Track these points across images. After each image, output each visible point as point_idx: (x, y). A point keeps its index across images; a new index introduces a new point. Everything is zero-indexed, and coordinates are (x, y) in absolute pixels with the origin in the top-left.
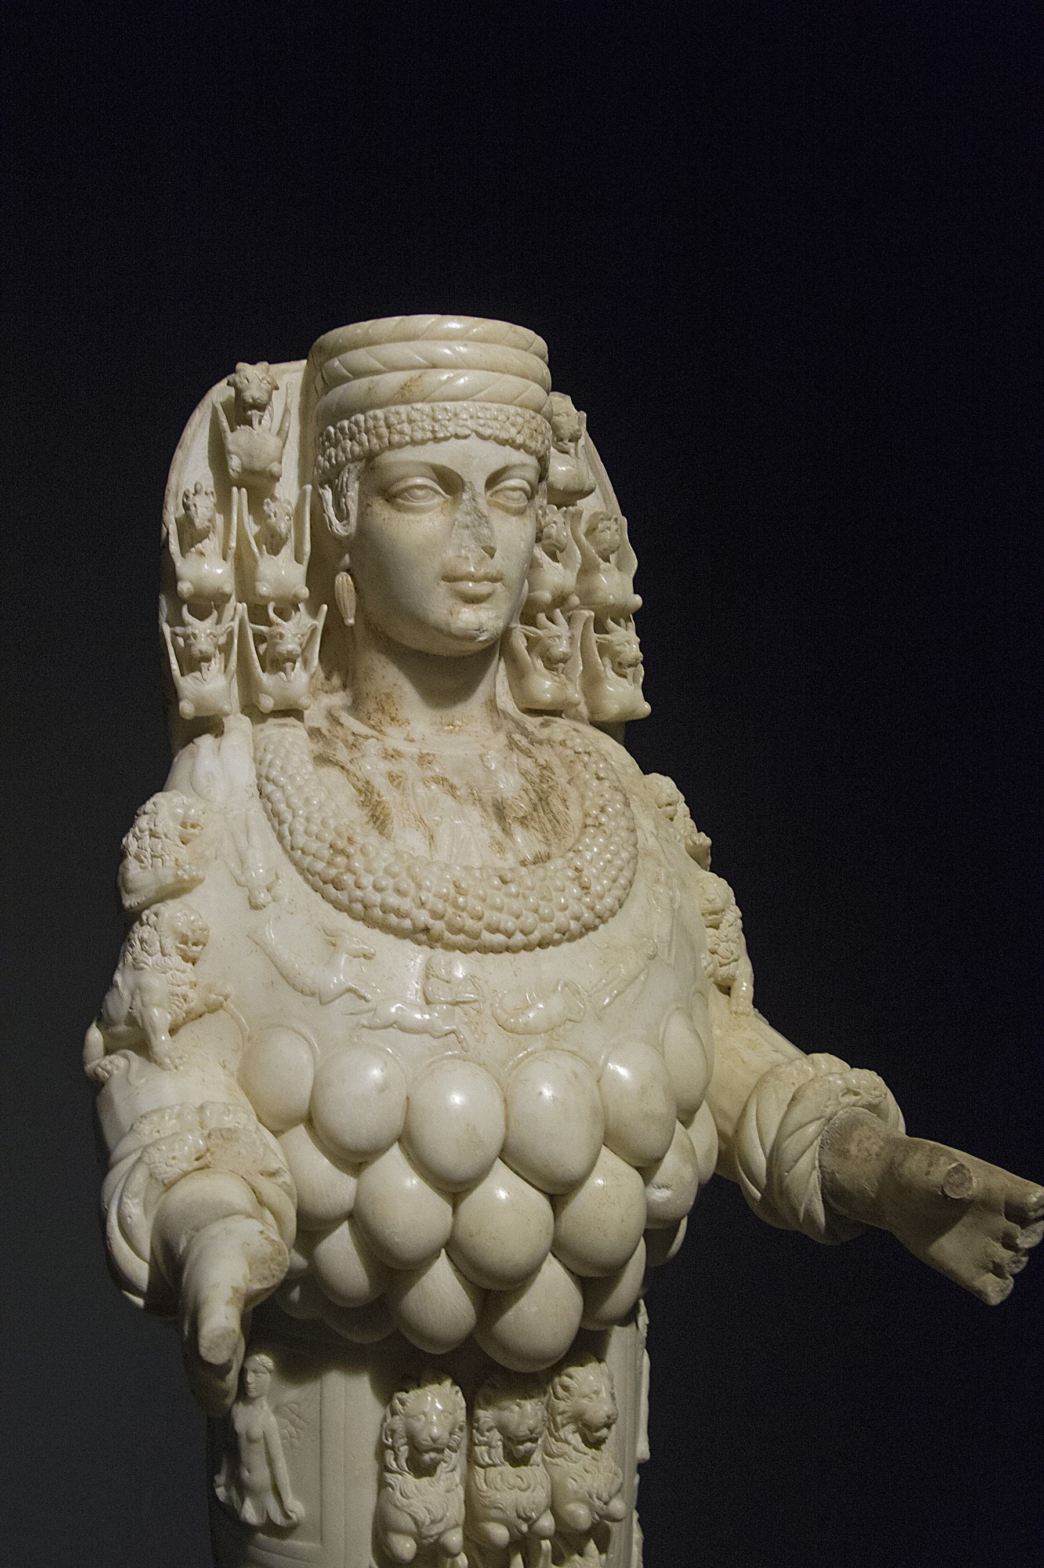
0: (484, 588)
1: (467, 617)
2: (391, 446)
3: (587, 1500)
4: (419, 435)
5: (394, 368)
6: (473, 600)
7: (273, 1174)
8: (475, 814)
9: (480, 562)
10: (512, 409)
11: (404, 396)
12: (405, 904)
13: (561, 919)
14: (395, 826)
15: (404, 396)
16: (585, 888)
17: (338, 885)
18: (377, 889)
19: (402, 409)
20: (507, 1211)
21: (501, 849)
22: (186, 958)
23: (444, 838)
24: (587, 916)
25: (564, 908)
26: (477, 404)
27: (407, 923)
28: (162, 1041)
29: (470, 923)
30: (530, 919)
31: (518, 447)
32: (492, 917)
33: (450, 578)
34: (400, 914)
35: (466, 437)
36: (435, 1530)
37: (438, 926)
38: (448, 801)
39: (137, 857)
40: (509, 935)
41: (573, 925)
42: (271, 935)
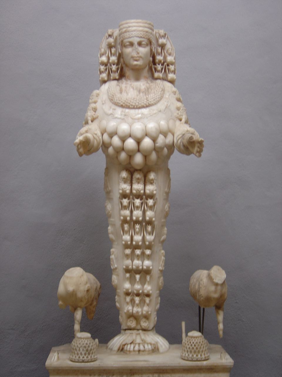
0: (138, 58)
1: (135, 63)
2: (124, 39)
3: (149, 190)
4: (127, 37)
5: (124, 28)
6: (136, 60)
7: (96, 134)
8: (135, 91)
9: (136, 55)
10: (141, 32)
11: (125, 32)
12: (120, 102)
13: (143, 104)
14: (123, 93)
15: (125, 32)
16: (147, 100)
17: (112, 100)
18: (117, 100)
19: (125, 34)
20: (130, 143)
21: (137, 96)
22: (94, 111)
23: (129, 94)
24: (147, 104)
25: (143, 103)
26: (136, 32)
27: (120, 105)
28: (90, 122)
29: (128, 104)
30: (137, 104)
31: (144, 38)
32: (131, 103)
33: (132, 57)
34: (120, 103)
35: (134, 37)
36: (125, 190)
37: (124, 105)
38: (132, 90)
39: (91, 99)
40: (134, 106)
41: (145, 105)
42: (104, 107)
